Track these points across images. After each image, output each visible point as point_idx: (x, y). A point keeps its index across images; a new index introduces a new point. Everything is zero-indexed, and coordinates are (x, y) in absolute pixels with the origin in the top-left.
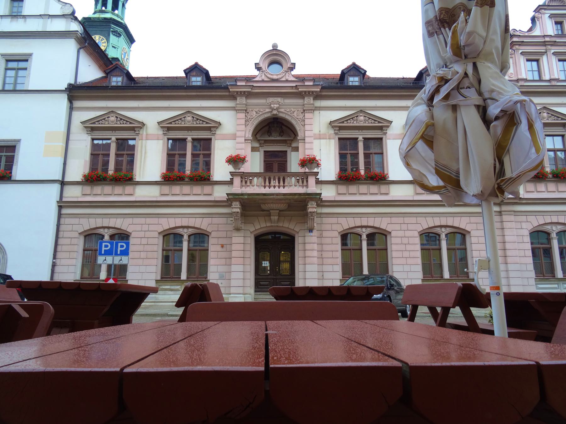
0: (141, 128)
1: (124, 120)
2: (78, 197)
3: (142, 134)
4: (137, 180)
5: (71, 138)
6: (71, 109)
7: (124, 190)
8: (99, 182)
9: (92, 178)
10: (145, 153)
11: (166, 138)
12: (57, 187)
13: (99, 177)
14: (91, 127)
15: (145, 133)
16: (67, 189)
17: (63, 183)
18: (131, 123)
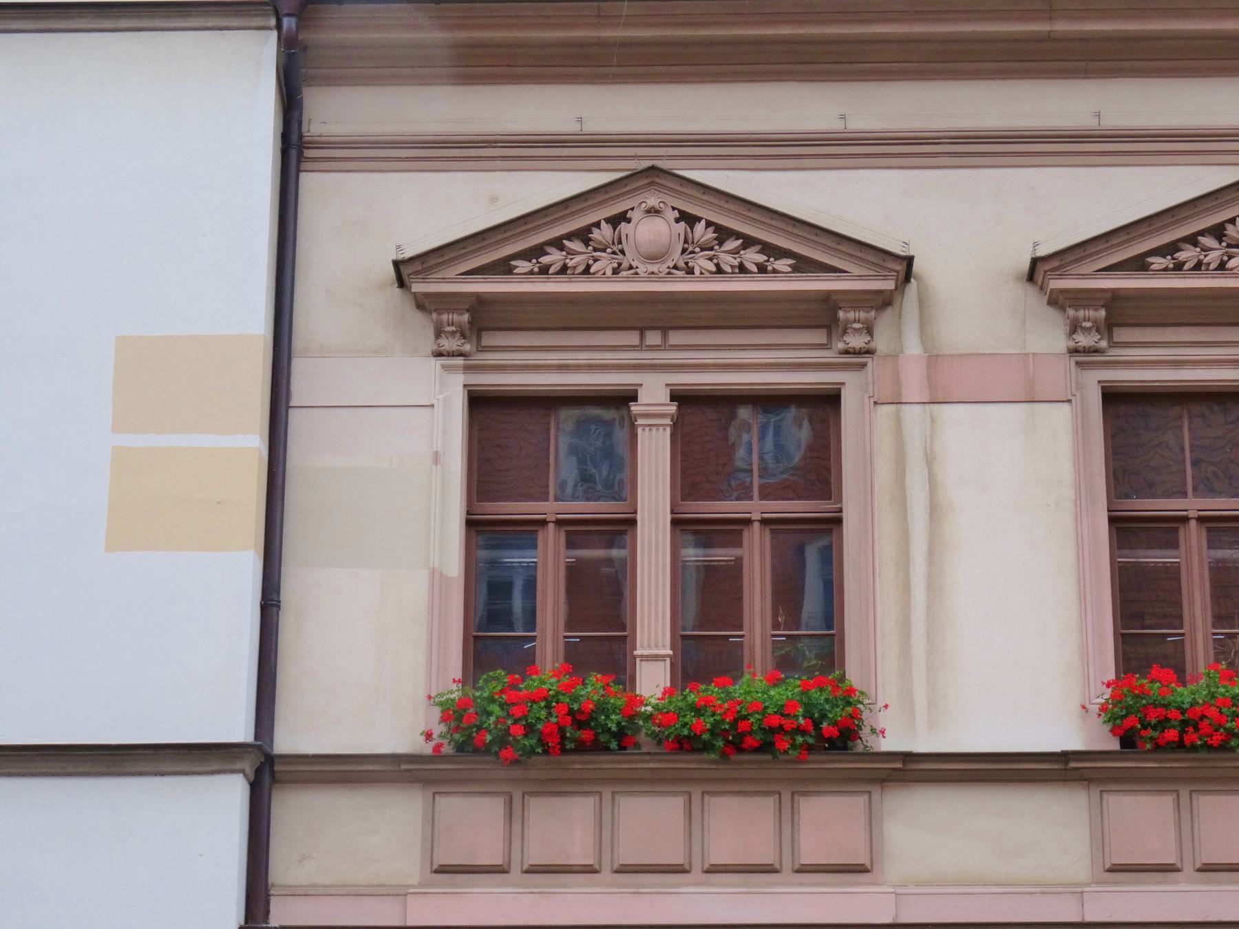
0: (883, 301)
1: (748, 242)
2: (400, 893)
3: (894, 357)
4: (888, 744)
5: (301, 388)
6: (294, 150)
7: (787, 820)
8: (577, 763)
9: (529, 729)
10: (935, 510)
11: (1092, 383)
12: (229, 794)
13: (581, 719)
14: (453, 295)
15: (913, 347)
16: (294, 810)
17: (266, 771)
18: (803, 265)
